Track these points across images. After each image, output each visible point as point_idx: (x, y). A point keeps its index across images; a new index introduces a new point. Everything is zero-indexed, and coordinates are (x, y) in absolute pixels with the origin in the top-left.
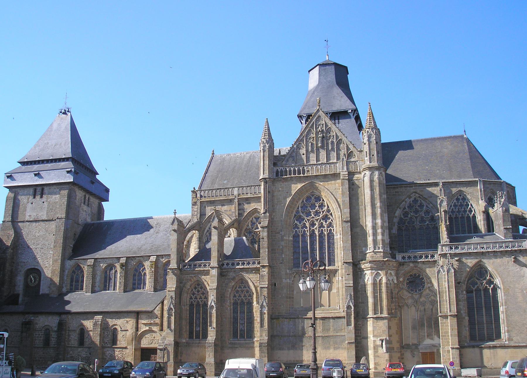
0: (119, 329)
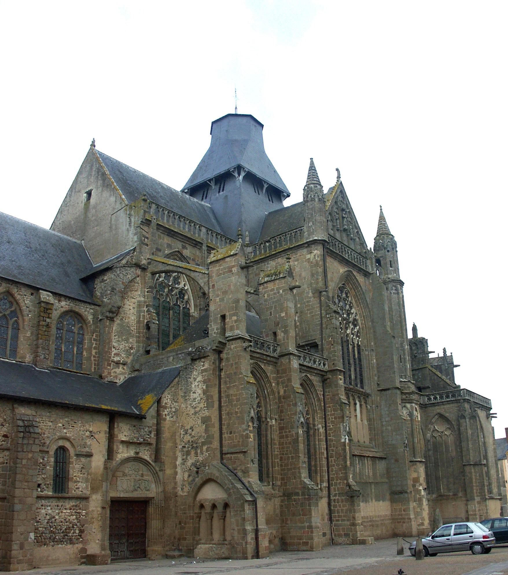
0: (72, 452)
